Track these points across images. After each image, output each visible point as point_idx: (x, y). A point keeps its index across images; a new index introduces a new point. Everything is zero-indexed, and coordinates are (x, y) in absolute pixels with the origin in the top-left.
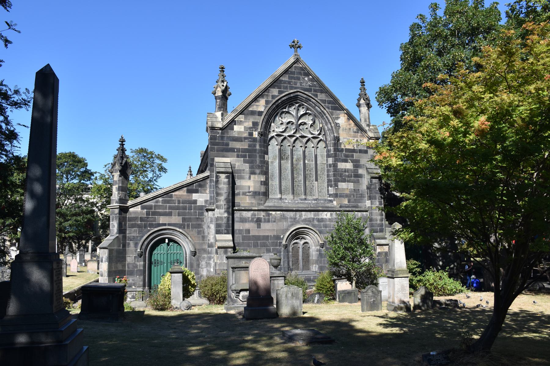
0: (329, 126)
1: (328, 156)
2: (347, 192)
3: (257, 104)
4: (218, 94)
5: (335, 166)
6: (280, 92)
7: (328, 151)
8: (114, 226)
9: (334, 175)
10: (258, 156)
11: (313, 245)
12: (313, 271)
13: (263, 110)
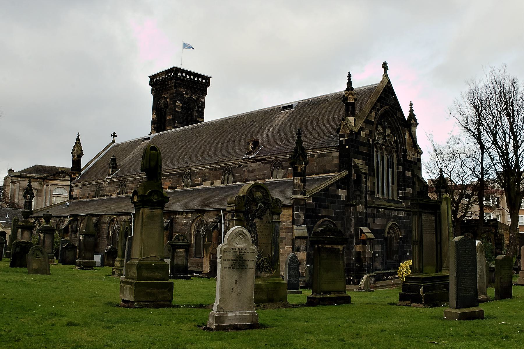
0: (401, 140)
1: (398, 165)
2: (409, 196)
3: (371, 115)
4: (350, 101)
5: (404, 173)
6: (382, 107)
7: (399, 160)
8: (300, 216)
9: (404, 181)
10: (372, 160)
11: (394, 238)
12: (394, 260)
13: (373, 121)
